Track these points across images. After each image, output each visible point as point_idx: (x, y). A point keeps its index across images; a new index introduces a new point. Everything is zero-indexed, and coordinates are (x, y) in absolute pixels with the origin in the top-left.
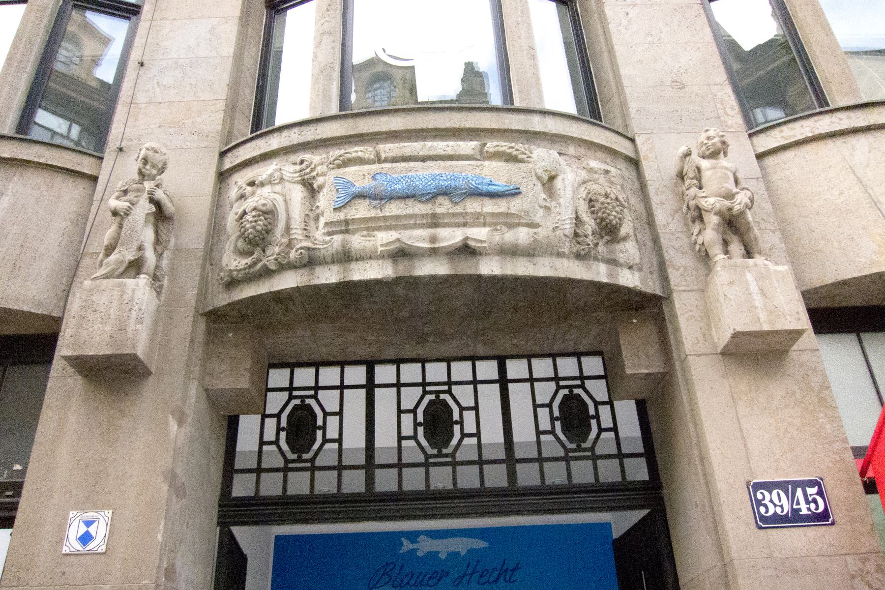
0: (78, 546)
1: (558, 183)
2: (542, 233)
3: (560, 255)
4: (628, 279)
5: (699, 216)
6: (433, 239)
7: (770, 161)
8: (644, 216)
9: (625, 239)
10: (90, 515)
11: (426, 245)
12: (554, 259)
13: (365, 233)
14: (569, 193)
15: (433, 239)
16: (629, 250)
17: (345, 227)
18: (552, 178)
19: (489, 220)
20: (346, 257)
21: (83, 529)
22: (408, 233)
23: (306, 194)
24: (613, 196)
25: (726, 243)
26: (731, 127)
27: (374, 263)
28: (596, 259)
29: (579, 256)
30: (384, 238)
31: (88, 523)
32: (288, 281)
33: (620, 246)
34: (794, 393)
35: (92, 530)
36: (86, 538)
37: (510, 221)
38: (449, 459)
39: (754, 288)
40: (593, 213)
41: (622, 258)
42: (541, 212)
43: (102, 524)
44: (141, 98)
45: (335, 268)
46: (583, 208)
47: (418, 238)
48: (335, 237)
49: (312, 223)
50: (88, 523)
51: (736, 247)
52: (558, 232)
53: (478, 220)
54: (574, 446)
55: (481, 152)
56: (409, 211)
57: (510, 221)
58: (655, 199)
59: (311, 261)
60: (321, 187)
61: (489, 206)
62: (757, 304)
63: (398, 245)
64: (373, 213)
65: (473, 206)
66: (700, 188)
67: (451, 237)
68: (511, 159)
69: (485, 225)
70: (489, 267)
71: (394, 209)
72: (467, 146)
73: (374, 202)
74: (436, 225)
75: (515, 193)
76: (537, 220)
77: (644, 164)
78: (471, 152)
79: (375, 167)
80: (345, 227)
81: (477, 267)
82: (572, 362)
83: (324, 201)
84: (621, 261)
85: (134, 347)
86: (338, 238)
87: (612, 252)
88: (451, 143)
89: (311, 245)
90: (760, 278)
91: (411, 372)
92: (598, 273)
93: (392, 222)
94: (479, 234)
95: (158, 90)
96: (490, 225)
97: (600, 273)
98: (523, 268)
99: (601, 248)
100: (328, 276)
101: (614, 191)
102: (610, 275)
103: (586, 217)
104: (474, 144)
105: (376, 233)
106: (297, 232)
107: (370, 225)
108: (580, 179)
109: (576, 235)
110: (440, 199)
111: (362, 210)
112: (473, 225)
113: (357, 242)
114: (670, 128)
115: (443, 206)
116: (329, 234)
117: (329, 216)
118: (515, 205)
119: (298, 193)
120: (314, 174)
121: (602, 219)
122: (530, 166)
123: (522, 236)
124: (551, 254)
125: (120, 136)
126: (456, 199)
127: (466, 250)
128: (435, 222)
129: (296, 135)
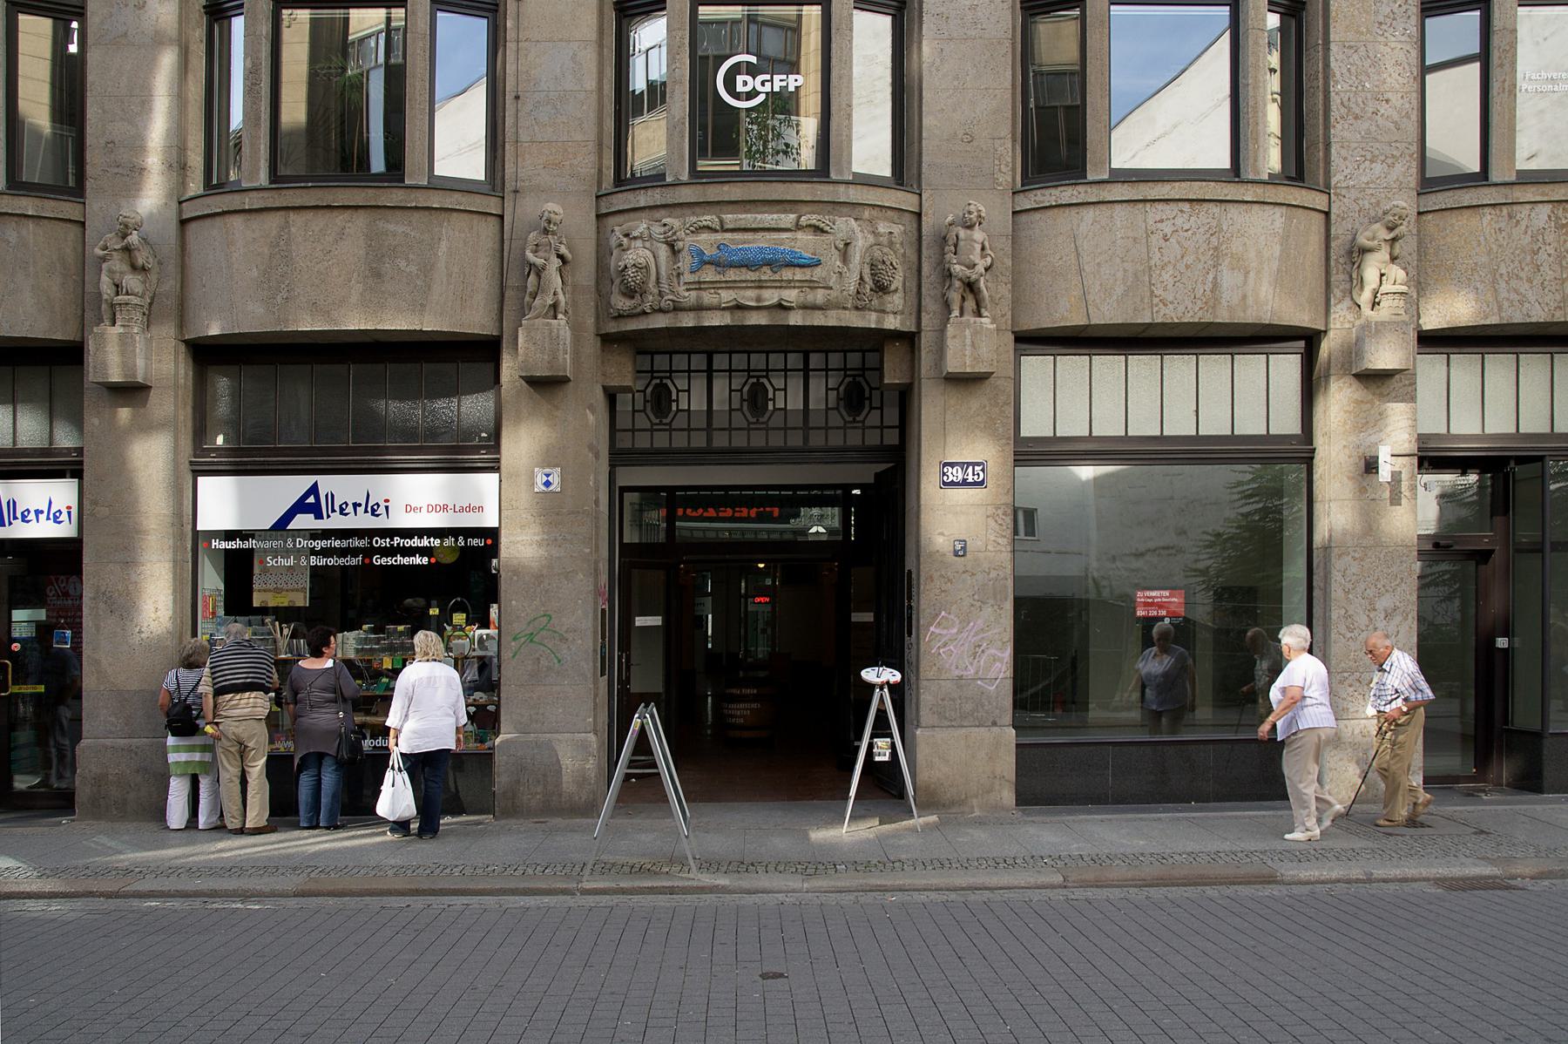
0: (544, 488)
1: (851, 248)
2: (834, 294)
3: (845, 308)
4: (891, 323)
5: (948, 275)
6: (758, 299)
7: (1023, 218)
8: (915, 267)
9: (896, 290)
10: (547, 470)
11: (753, 304)
12: (840, 311)
13: (713, 291)
14: (858, 257)
15: (758, 299)
16: (896, 301)
17: (699, 286)
18: (847, 245)
19: (797, 284)
20: (699, 308)
21: (545, 479)
22: (742, 292)
23: (669, 253)
24: (888, 263)
25: (963, 299)
26: (1001, 185)
27: (719, 313)
28: (870, 310)
29: (857, 308)
30: (727, 296)
31: (548, 475)
32: (660, 322)
33: (888, 298)
34: (985, 407)
35: (550, 479)
36: (547, 484)
37: (812, 285)
38: (764, 426)
39: (968, 341)
40: (872, 274)
41: (889, 307)
42: (835, 277)
43: (556, 476)
44: (524, 137)
45: (692, 314)
46: (867, 271)
47: (748, 297)
48: (691, 292)
49: (675, 280)
50: (548, 475)
51: (970, 304)
52: (845, 293)
53: (789, 284)
54: (851, 419)
55: (797, 224)
56: (743, 278)
57: (812, 285)
58: (925, 252)
59: (677, 308)
60: (679, 251)
61: (799, 275)
62: (967, 353)
63: (735, 303)
64: (717, 278)
65: (787, 274)
66: (955, 254)
67: (771, 297)
68: (818, 230)
69: (794, 287)
70: (795, 319)
71: (732, 275)
72: (788, 219)
73: (718, 269)
74: (761, 287)
75: (818, 264)
76: (831, 284)
77: (924, 218)
78: (789, 226)
79: (719, 236)
80: (699, 286)
81: (787, 318)
82: (858, 355)
83: (685, 262)
84: (888, 310)
85: (565, 370)
86: (694, 294)
87: (882, 304)
88: (775, 216)
89: (675, 298)
90: (975, 333)
91: (739, 361)
92: (869, 321)
93: (731, 285)
94: (791, 296)
95: (536, 128)
96: (798, 287)
97: (870, 321)
98: (818, 320)
99: (875, 302)
100: (688, 321)
101: (892, 258)
102: (878, 322)
103: (867, 278)
104: (793, 216)
105: (720, 291)
106: (665, 287)
107: (715, 286)
108: (867, 244)
109: (858, 292)
110: (765, 269)
111: (709, 275)
112: (786, 288)
113: (708, 298)
114: (952, 185)
115: (766, 274)
116: (688, 290)
117: (688, 277)
118: (818, 273)
119: (663, 252)
120: (675, 237)
121: (878, 281)
122: (829, 237)
123: (819, 296)
124: (839, 308)
125: (514, 177)
126: (775, 269)
127: (781, 307)
128: (760, 285)
129: (658, 196)
